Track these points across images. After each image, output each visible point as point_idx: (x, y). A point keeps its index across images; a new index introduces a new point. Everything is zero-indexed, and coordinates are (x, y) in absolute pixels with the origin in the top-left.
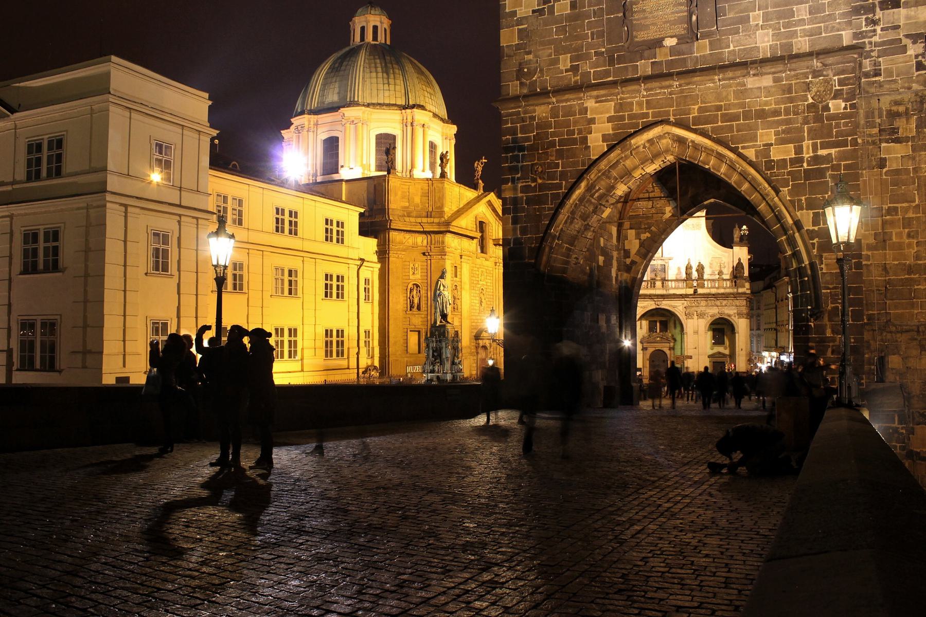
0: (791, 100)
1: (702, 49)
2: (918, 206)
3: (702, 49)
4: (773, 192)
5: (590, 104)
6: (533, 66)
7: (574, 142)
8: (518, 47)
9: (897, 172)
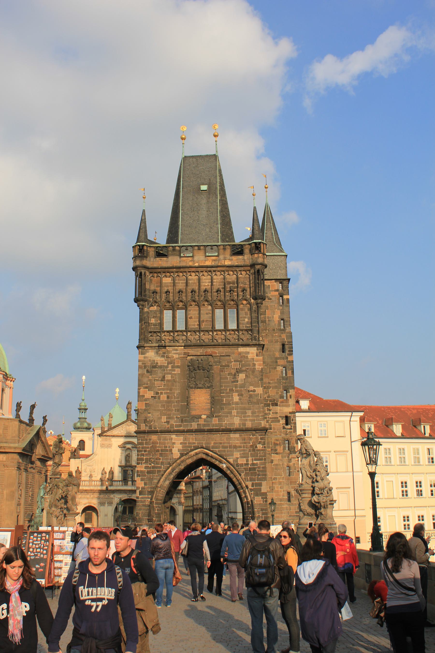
0: (245, 443)
1: (215, 421)
2: (283, 477)
3: (215, 421)
4: (238, 475)
5: (174, 436)
6: (151, 419)
7: (167, 450)
8: (145, 410)
9: (277, 465)
